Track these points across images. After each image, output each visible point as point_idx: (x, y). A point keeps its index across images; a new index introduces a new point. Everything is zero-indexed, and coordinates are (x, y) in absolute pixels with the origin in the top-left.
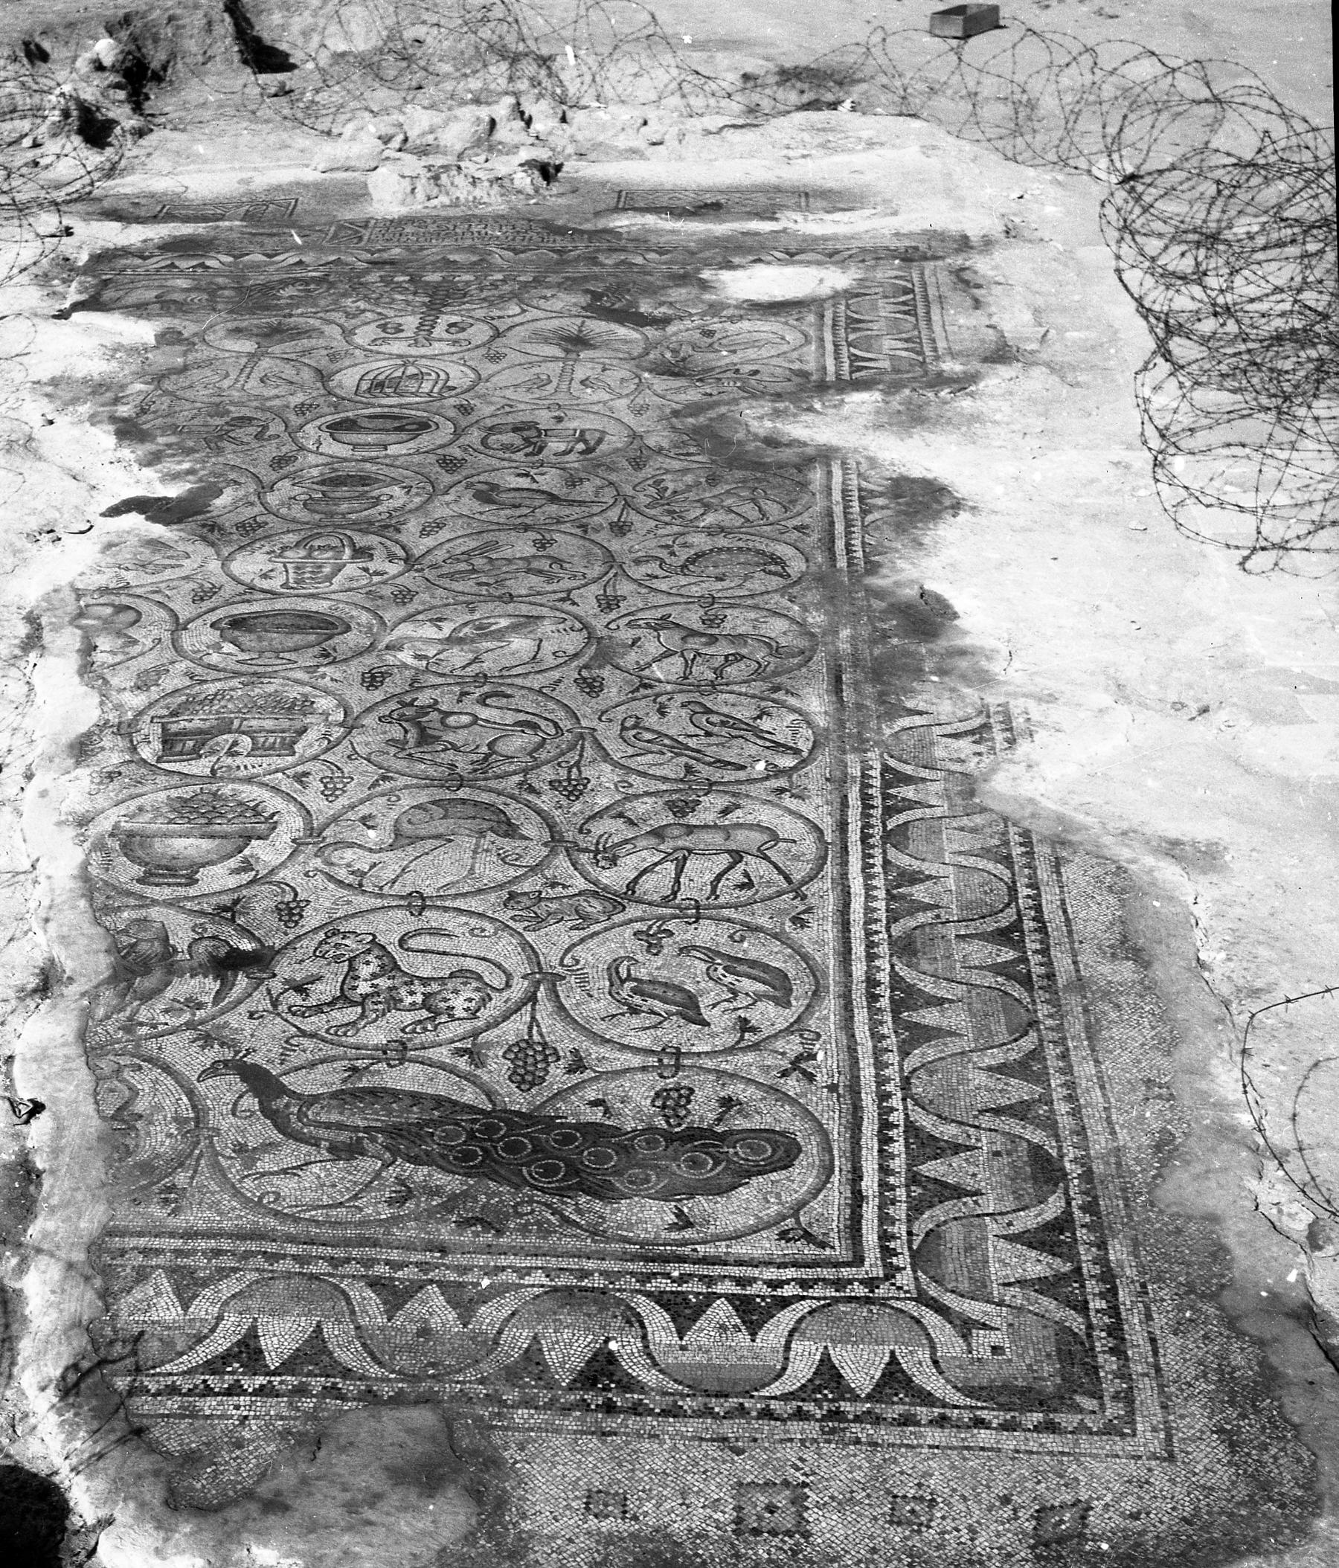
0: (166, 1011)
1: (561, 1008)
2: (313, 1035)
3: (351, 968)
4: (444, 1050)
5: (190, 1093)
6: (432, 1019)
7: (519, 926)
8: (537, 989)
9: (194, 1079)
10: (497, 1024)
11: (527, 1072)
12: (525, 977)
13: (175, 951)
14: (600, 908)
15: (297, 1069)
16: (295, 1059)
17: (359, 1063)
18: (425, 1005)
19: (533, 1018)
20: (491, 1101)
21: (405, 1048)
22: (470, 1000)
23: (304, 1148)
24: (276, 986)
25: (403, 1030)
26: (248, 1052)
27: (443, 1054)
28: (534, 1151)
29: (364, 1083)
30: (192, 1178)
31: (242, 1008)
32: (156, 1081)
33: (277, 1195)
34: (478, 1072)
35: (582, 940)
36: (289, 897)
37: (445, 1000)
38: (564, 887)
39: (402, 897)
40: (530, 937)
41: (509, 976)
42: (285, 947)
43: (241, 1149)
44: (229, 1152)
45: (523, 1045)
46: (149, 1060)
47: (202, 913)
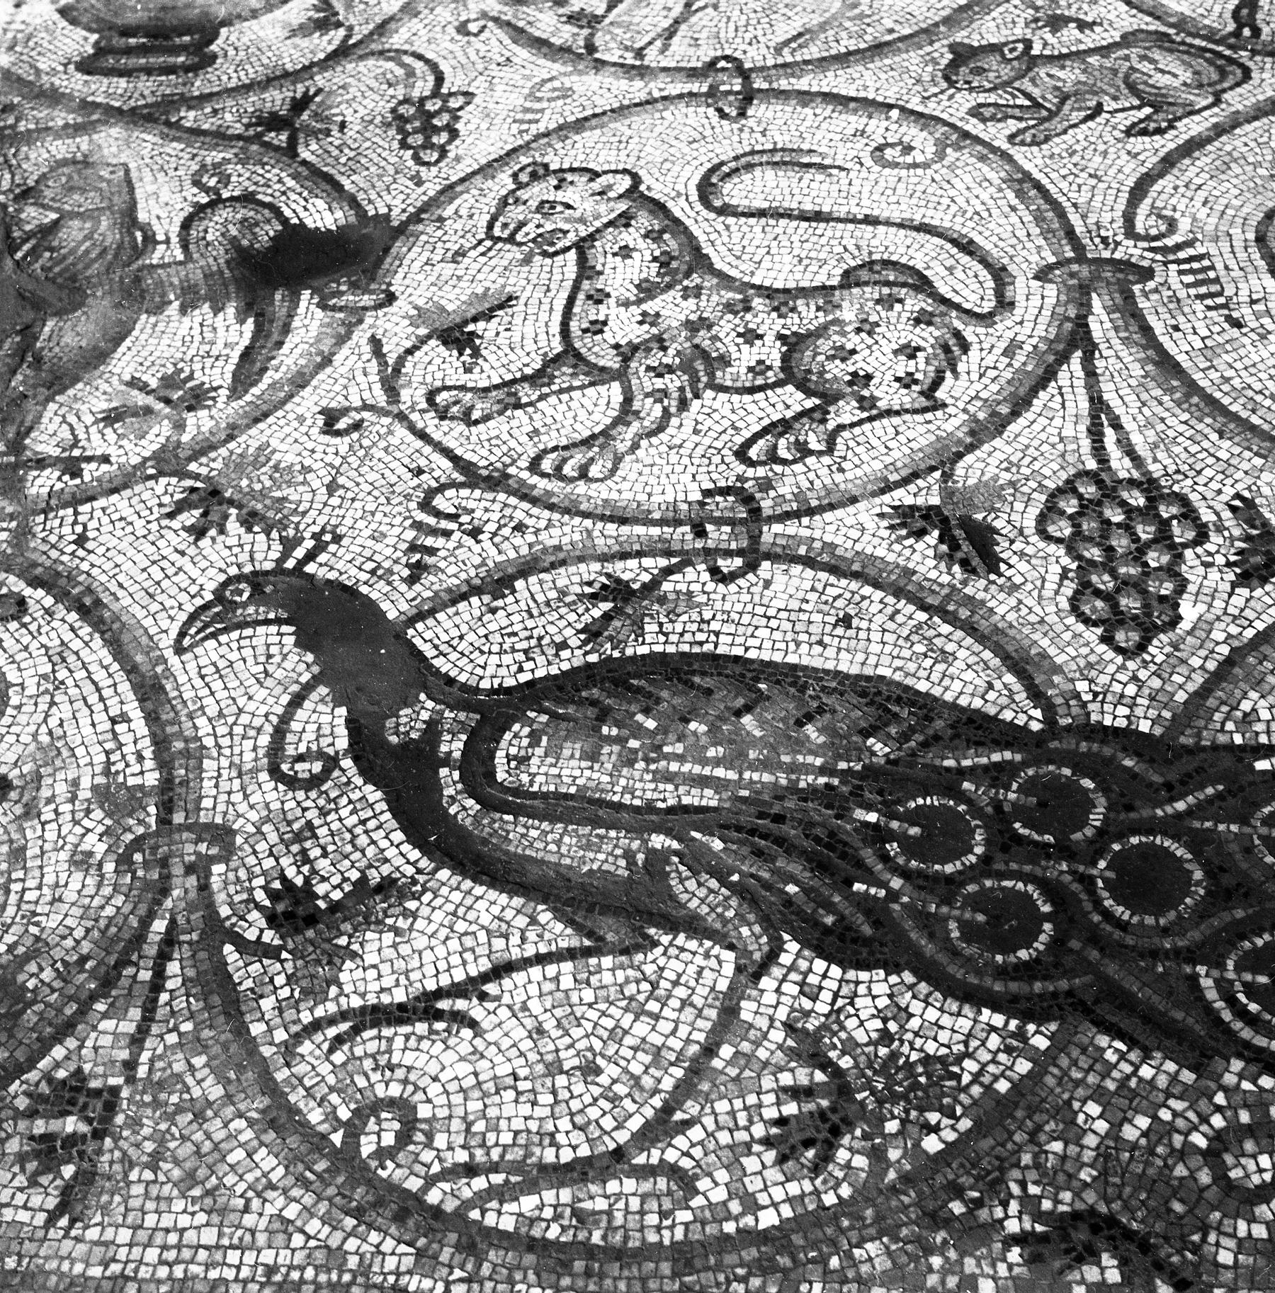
0: (111, 418)
1: (1166, 365)
2: (496, 481)
3: (586, 270)
4: (865, 512)
5: (150, 691)
6: (817, 415)
7: (997, 134)
8: (1086, 307)
9: (166, 642)
10: (997, 425)
11: (1125, 584)
12: (1043, 275)
13: (150, 240)
14: (1186, 76)
15: (458, 597)
16: (459, 560)
17: (632, 572)
18: (791, 374)
19: (1098, 404)
20: (1036, 695)
21: (755, 512)
22: (910, 351)
23: (491, 904)
24: (395, 327)
25: (741, 454)
26: (320, 547)
27: (860, 530)
28: (1220, 895)
29: (651, 643)
30: (137, 1041)
31: (308, 403)
32: (59, 657)
33: (404, 1109)
34: (976, 588)
35: (1168, 163)
36: (423, 86)
37: (845, 354)
38: (1082, 25)
39: (693, 73)
40: (1030, 160)
41: (1000, 275)
42: (416, 218)
43: (295, 911)
44: (255, 927)
45: (1089, 490)
46: (51, 580)
47: (220, 137)
